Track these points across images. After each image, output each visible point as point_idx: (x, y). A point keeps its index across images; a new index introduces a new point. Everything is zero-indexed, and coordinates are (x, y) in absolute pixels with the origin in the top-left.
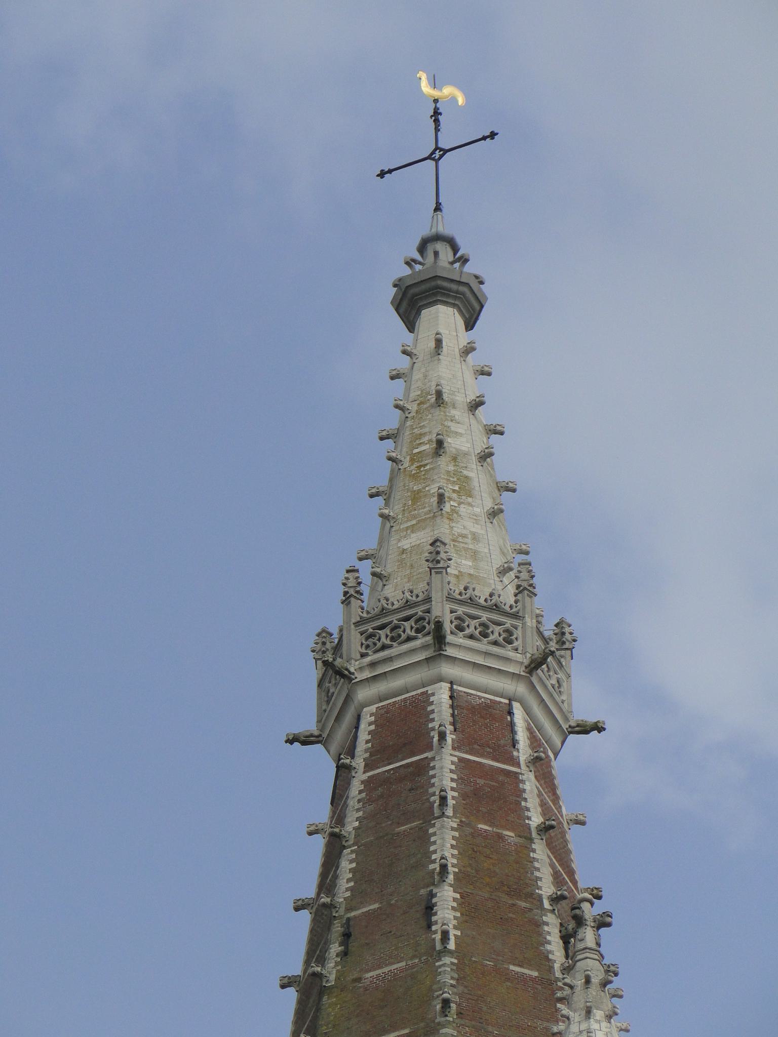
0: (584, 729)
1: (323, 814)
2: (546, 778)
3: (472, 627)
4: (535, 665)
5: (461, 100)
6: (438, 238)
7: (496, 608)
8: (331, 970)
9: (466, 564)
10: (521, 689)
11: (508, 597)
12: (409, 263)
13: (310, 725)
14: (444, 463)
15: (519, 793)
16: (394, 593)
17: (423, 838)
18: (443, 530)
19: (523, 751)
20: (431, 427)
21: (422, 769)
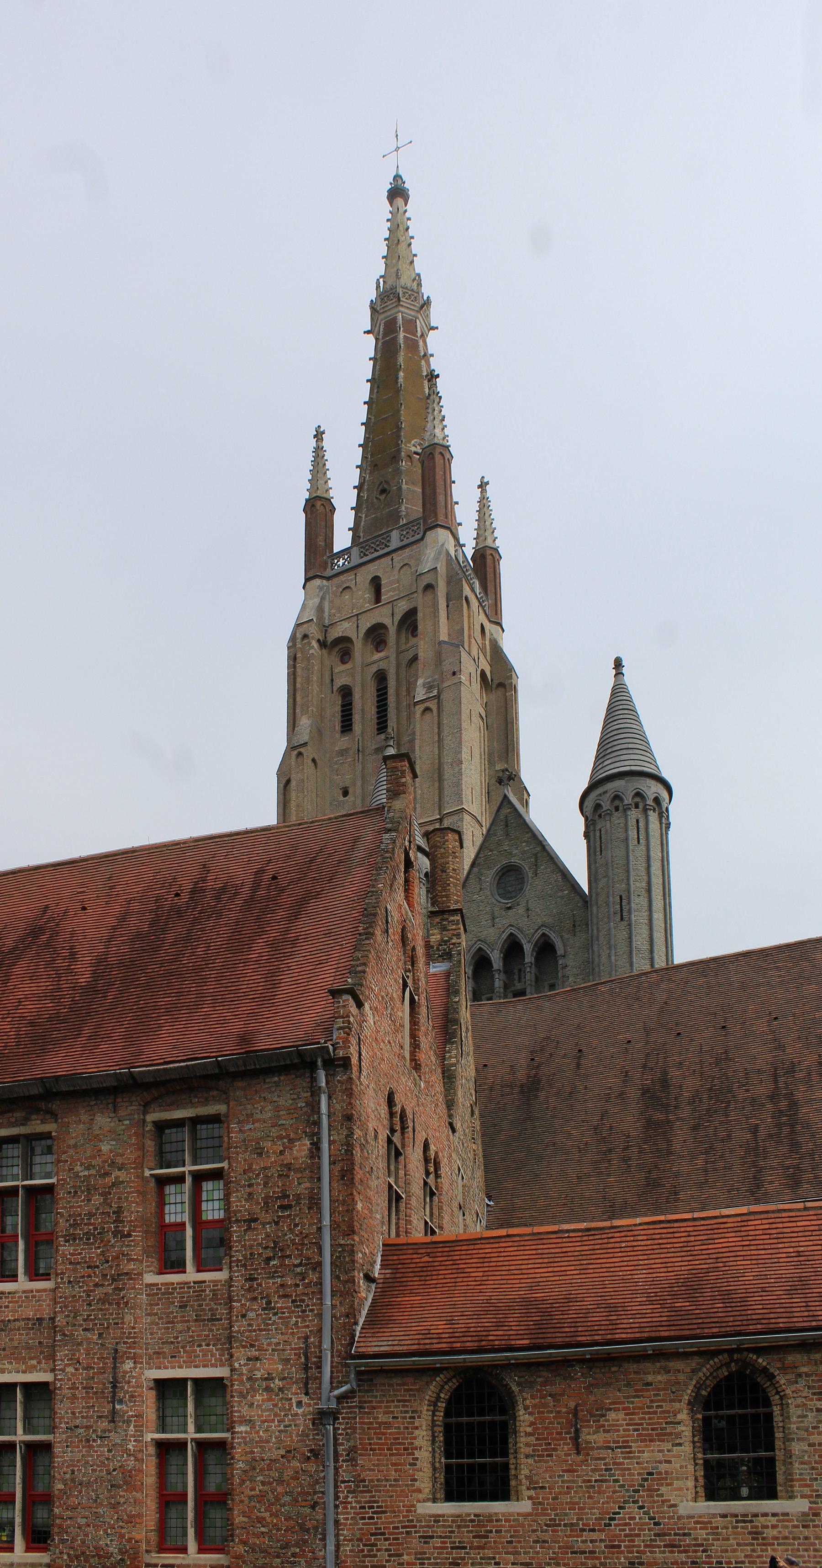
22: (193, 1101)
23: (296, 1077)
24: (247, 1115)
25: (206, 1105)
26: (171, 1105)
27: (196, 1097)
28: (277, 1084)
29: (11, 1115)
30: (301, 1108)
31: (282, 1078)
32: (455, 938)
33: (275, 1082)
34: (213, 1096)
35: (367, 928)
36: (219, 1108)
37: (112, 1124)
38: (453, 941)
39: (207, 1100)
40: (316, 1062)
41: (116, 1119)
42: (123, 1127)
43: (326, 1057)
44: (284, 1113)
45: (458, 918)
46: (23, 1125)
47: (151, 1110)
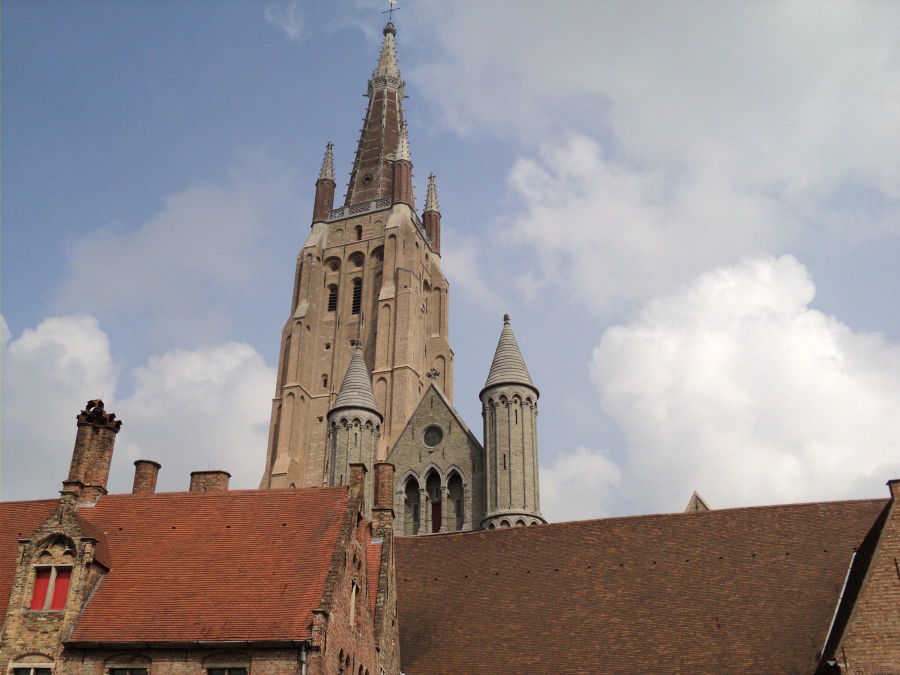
0: (406, 97)
1: (367, 106)
2: (400, 104)
3: (391, 81)
4: (399, 87)
5: (395, 3)
6: (390, 23)
7: (395, 78)
8: (367, 130)
9: (391, 71)
10: (397, 90)
11: (396, 77)
12: (386, 26)
13: (366, 93)
14: (389, 56)
15: (396, 106)
16: (380, 75)
17: (381, 111)
18: (388, 66)
19: (397, 99)
20: (387, 51)
21: (382, 101)
22: (231, 659)
23: (290, 653)
24: (261, 670)
25: (239, 662)
26: (218, 660)
27: (233, 657)
28: (279, 656)
29: (123, 656)
30: (291, 670)
31: (282, 653)
32: (387, 525)
33: (278, 655)
34: (243, 658)
35: (334, 568)
36: (247, 665)
37: (184, 668)
38: (386, 527)
39: (239, 659)
40: (301, 647)
41: (186, 666)
42: (190, 670)
43: (307, 645)
44: (282, 671)
45: (390, 513)
46: (130, 662)
47: (207, 662)
